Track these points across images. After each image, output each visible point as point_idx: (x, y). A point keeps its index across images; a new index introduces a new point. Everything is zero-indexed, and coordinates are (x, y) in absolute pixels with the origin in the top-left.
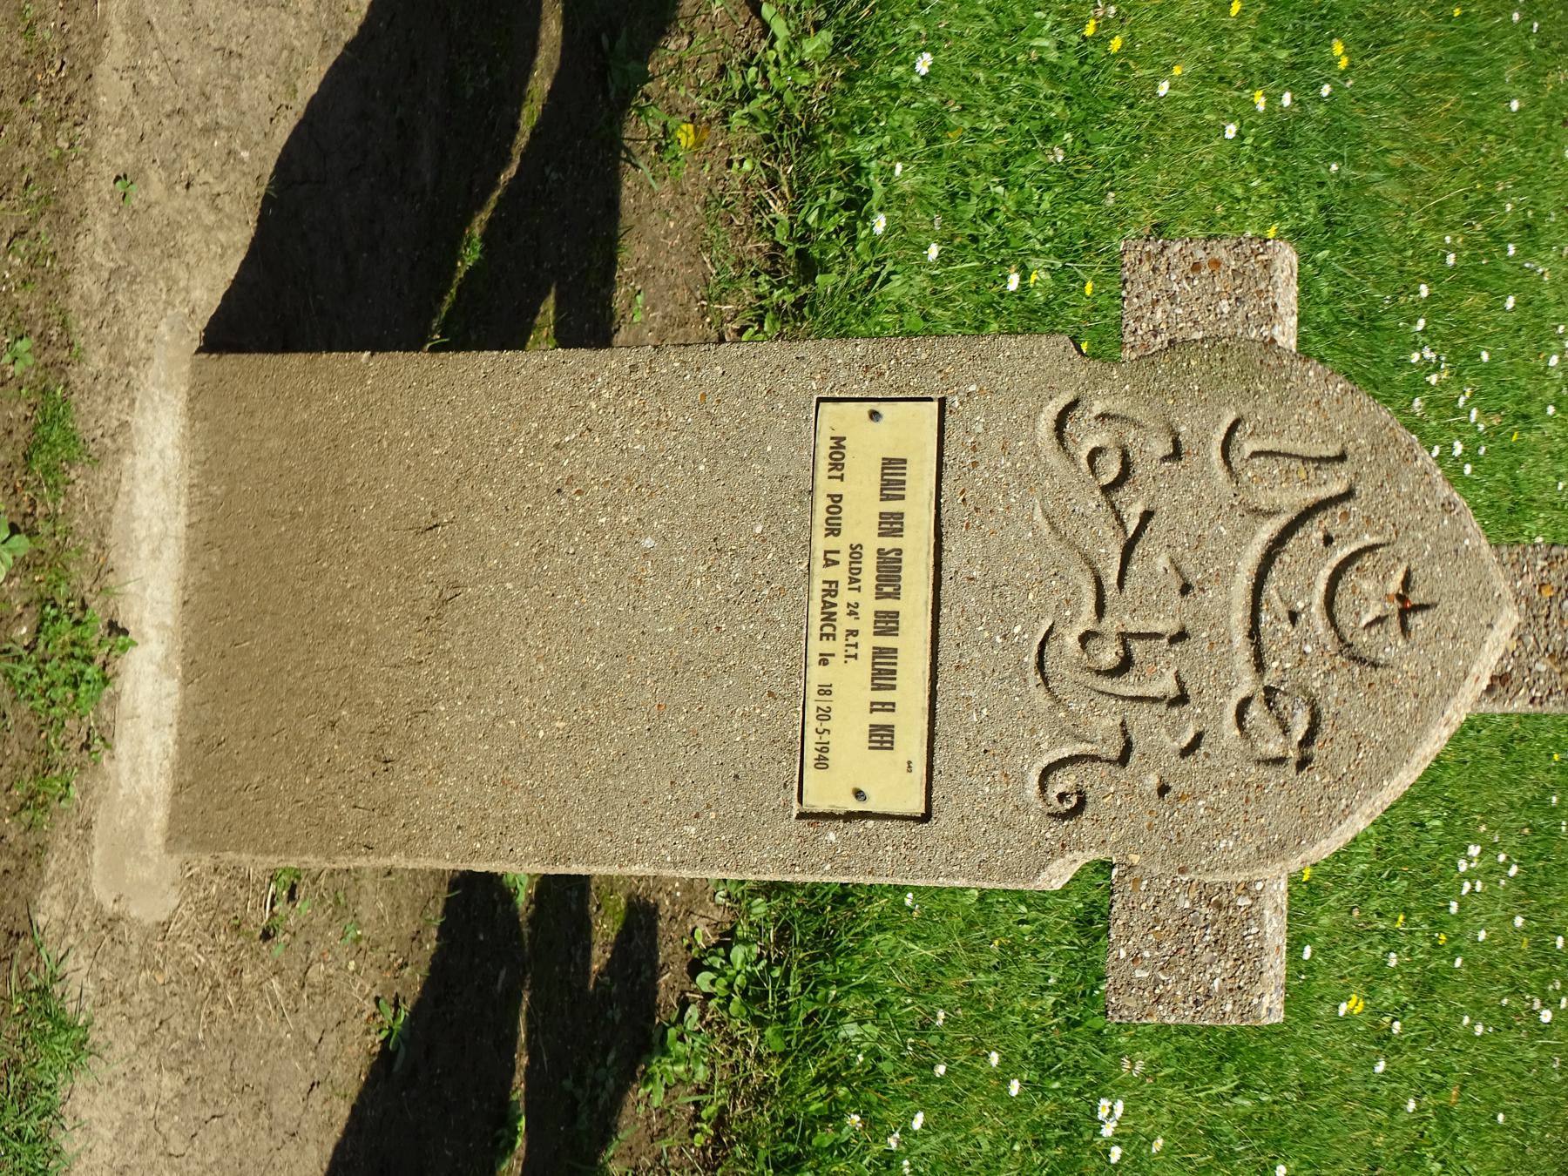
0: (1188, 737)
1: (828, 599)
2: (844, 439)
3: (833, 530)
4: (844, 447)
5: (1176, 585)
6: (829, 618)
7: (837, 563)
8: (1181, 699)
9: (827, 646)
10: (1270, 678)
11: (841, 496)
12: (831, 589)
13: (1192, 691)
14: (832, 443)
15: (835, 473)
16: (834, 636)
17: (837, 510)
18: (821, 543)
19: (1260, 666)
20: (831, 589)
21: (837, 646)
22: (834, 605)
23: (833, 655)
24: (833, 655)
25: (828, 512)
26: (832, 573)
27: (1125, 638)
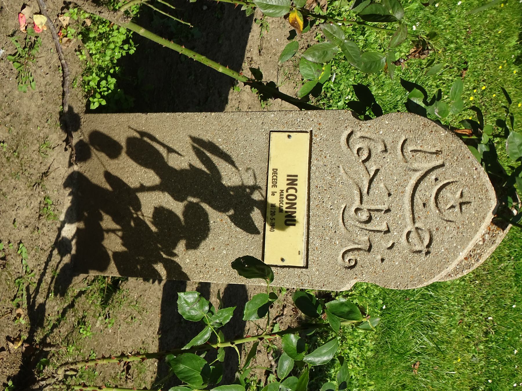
0: (390, 245)
5: (386, 194)
8: (388, 231)
10: (417, 225)
13: (391, 229)
19: (414, 220)
27: (369, 210)
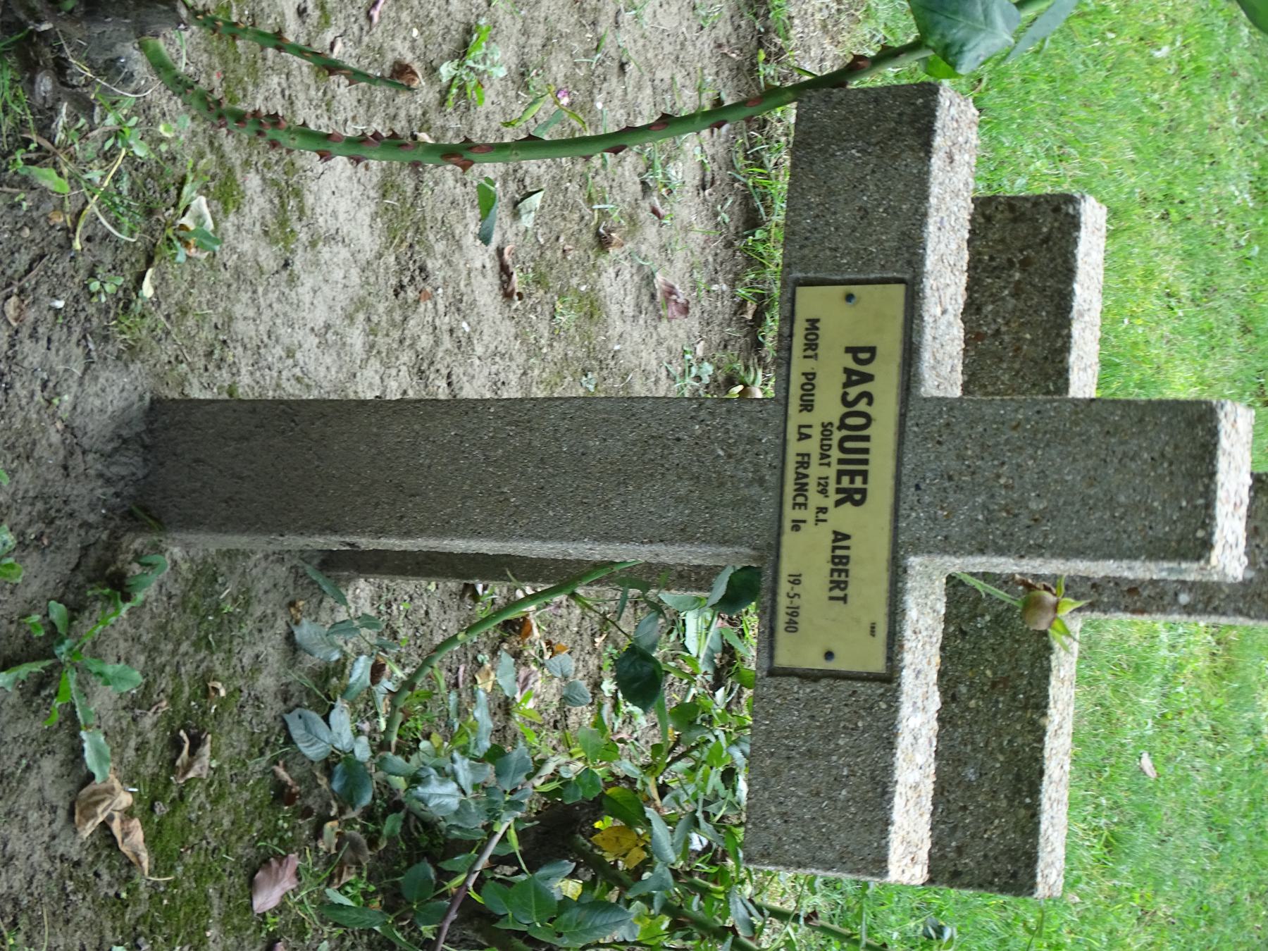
1: (801, 470)
2: (817, 320)
3: (807, 406)
4: (817, 329)
6: (801, 489)
7: (808, 436)
9: (799, 514)
11: (814, 374)
12: (804, 461)
14: (807, 325)
15: (810, 353)
16: (805, 505)
17: (809, 387)
18: (796, 417)
20: (804, 461)
21: (809, 514)
22: (806, 476)
23: (804, 521)
24: (804, 521)
25: (802, 387)
26: (805, 446)
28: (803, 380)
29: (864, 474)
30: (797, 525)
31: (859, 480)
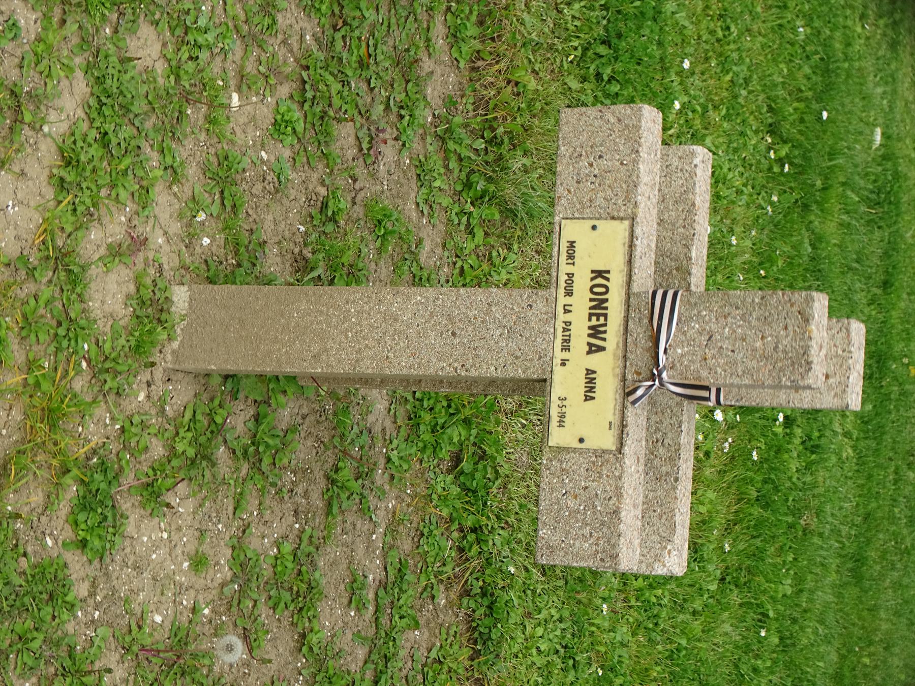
3: (569, 293)
6: (566, 341)
7: (570, 311)
14: (568, 244)
15: (570, 261)
18: (562, 300)
26: (568, 317)
28: (566, 277)
29: (605, 316)
30: (563, 364)
31: (602, 319)
